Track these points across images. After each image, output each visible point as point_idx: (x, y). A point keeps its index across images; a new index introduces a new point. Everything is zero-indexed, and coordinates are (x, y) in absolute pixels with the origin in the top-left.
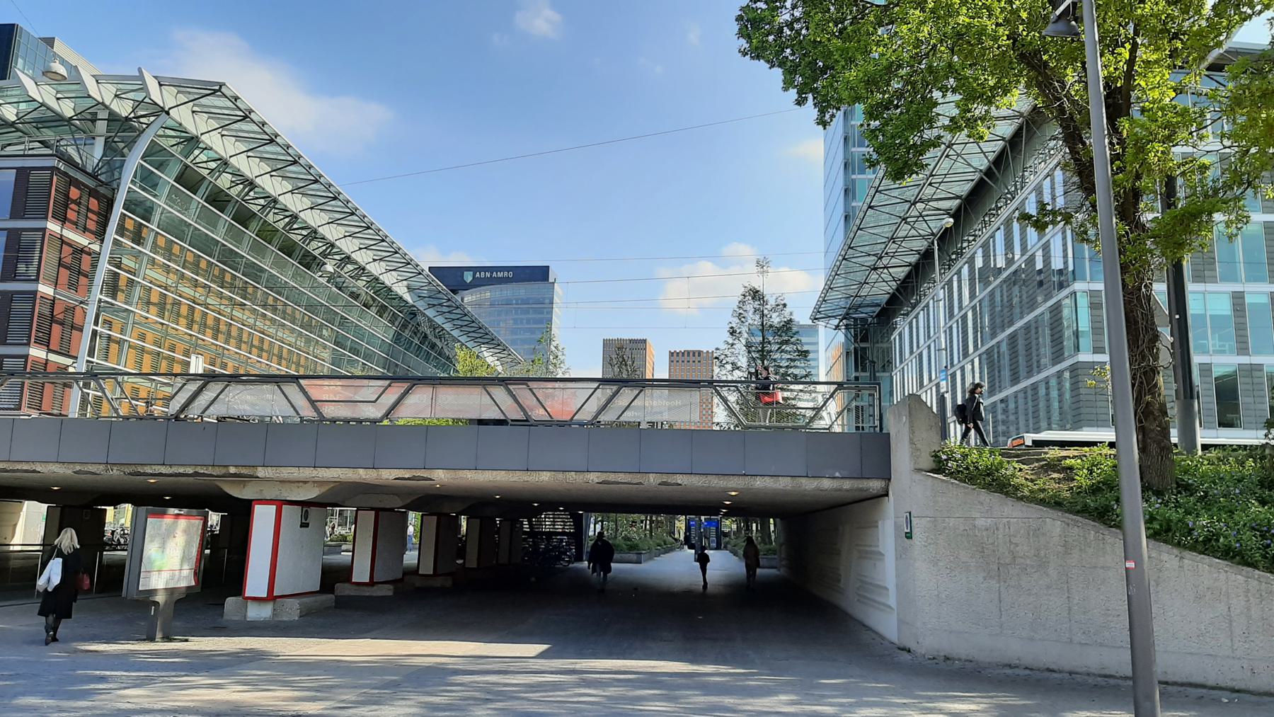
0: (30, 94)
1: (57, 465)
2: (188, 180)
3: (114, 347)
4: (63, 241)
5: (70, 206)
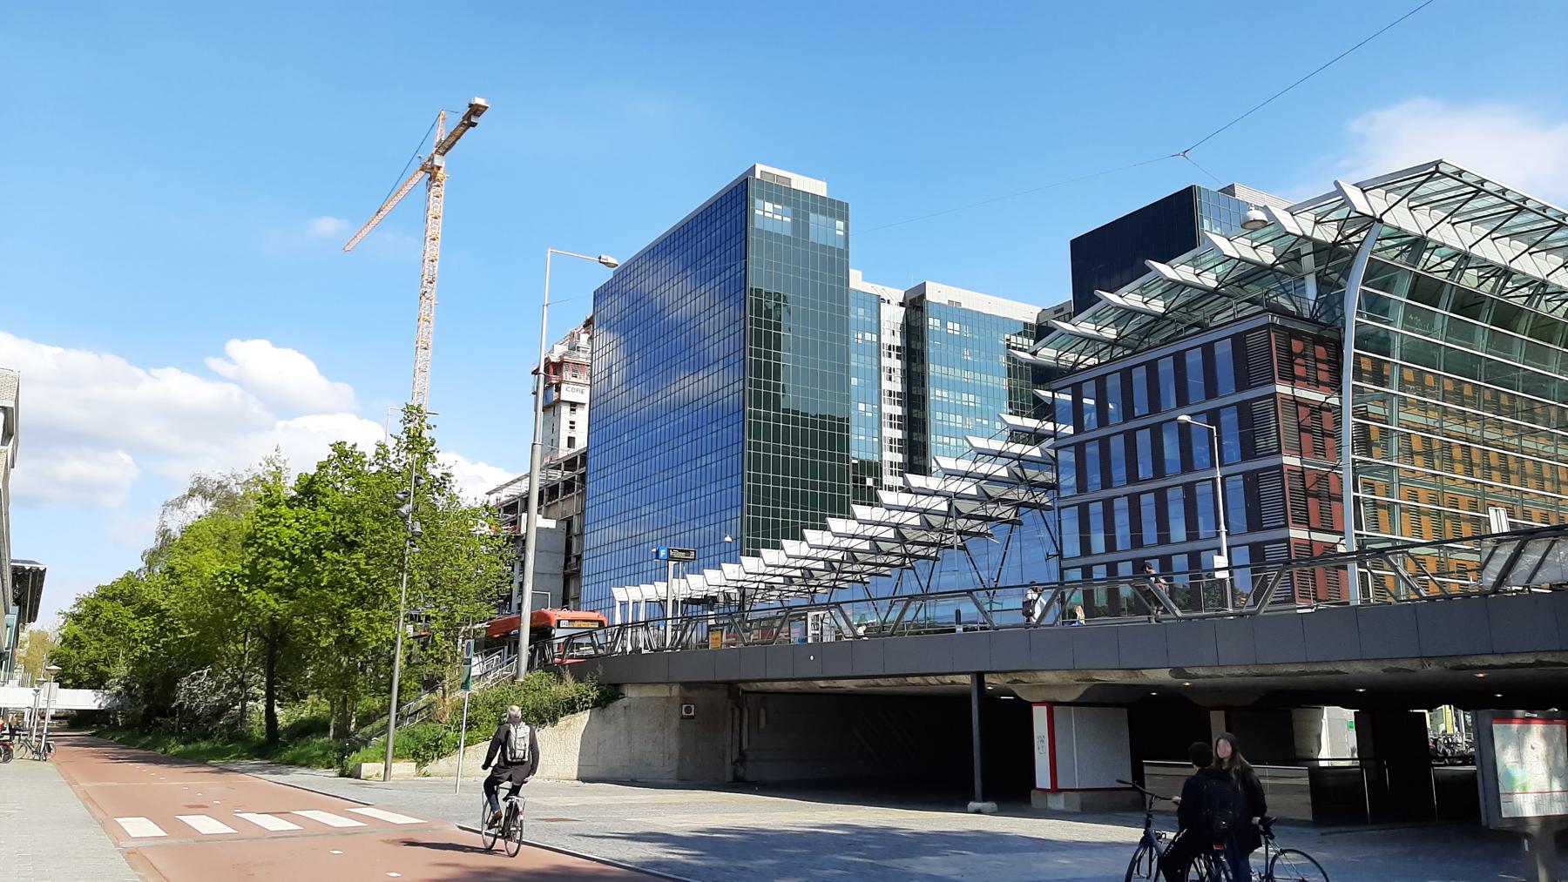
0: (1225, 253)
1: (1362, 663)
2: (1425, 290)
3: (1382, 513)
4: (1297, 402)
5: (1297, 361)
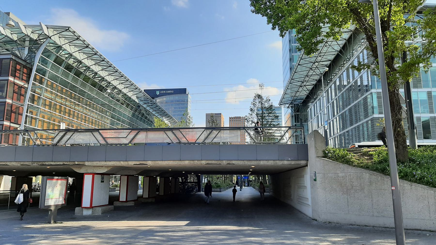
0: (1, 32)
2: (58, 61)
3: (33, 120)
4: (14, 84)
